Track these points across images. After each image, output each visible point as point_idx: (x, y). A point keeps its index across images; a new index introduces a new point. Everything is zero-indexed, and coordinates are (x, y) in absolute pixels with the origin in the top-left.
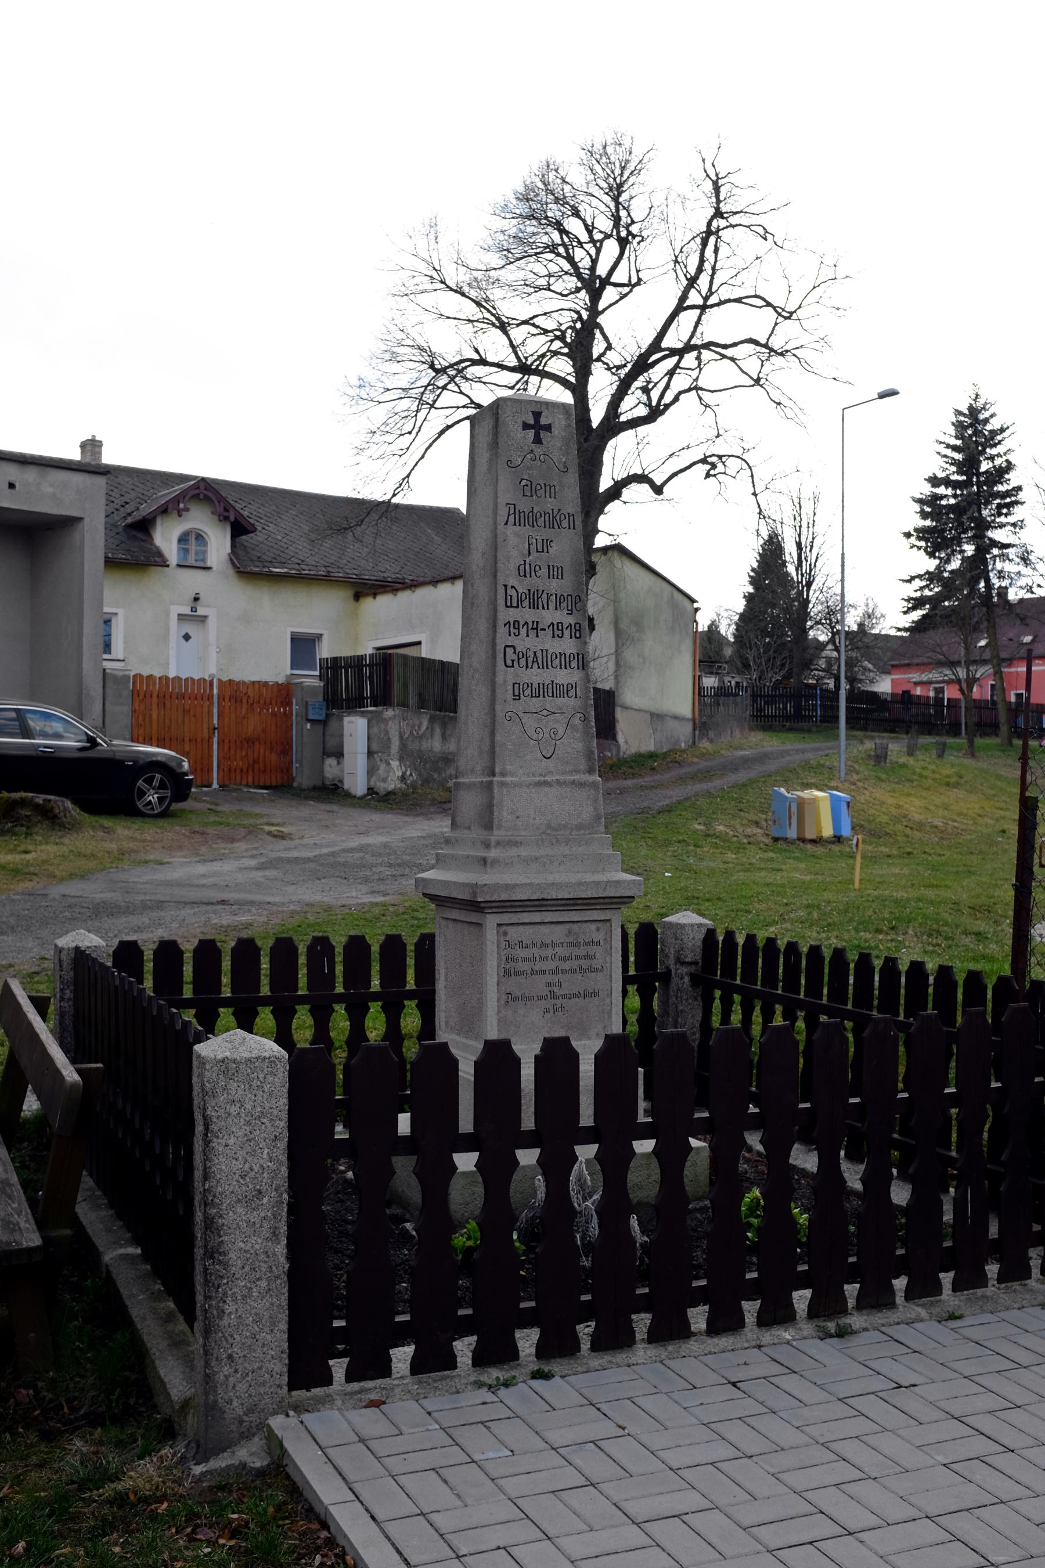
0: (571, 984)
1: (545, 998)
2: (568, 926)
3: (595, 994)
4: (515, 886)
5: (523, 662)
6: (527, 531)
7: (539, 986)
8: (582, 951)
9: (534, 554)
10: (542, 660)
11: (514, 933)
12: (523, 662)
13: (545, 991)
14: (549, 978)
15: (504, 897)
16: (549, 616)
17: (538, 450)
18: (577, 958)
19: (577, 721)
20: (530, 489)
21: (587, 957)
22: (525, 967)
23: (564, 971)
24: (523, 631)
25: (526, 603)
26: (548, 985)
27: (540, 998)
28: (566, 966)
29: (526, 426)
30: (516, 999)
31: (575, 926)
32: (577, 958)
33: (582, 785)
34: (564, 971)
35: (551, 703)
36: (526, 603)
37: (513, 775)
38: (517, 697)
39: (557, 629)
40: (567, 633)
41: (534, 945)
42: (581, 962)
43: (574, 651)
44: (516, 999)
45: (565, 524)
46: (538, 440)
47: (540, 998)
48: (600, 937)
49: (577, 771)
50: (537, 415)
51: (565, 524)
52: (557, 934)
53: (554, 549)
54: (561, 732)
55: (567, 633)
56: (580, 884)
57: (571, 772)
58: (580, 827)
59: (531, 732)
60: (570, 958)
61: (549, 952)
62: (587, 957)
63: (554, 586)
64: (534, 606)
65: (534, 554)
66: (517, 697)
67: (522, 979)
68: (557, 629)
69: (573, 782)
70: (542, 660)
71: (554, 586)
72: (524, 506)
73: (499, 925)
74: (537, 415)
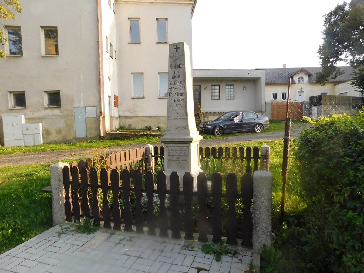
0: (182, 158)
1: (176, 160)
2: (181, 147)
3: (186, 161)
4: (166, 139)
5: (173, 95)
6: (174, 69)
7: (175, 158)
8: (183, 152)
9: (175, 74)
10: (177, 94)
11: (170, 148)
12: (173, 95)
13: (176, 159)
14: (177, 157)
15: (164, 141)
16: (178, 86)
17: (177, 53)
18: (183, 153)
19: (184, 106)
20: (175, 61)
21: (184, 153)
22: (172, 154)
23: (180, 156)
24: (173, 89)
25: (174, 84)
26: (177, 158)
27: (175, 160)
28: (180, 154)
29: (174, 49)
30: (170, 160)
31: (182, 147)
32: (183, 153)
33: (184, 119)
34: (180, 156)
35: (178, 103)
36: (174, 84)
37: (171, 117)
38: (172, 102)
39: (180, 88)
40: (182, 88)
41: (174, 150)
42: (183, 154)
43: (183, 92)
44: (170, 160)
45: (182, 66)
46: (177, 51)
47: (175, 160)
48: (187, 149)
49: (183, 116)
50: (177, 46)
51: (182, 66)
52: (178, 148)
53: (180, 72)
54: (180, 108)
55: (182, 88)
56: (179, 139)
57: (182, 116)
58: (184, 127)
59: (174, 109)
60: (181, 153)
61: (177, 152)
62: (184, 153)
63: (179, 79)
64: (175, 84)
65: (175, 74)
66: (172, 102)
67: (172, 157)
68: (180, 88)
69: (182, 118)
70: (177, 94)
71: (179, 79)
72: (174, 64)
73: (166, 146)
74: (177, 46)
